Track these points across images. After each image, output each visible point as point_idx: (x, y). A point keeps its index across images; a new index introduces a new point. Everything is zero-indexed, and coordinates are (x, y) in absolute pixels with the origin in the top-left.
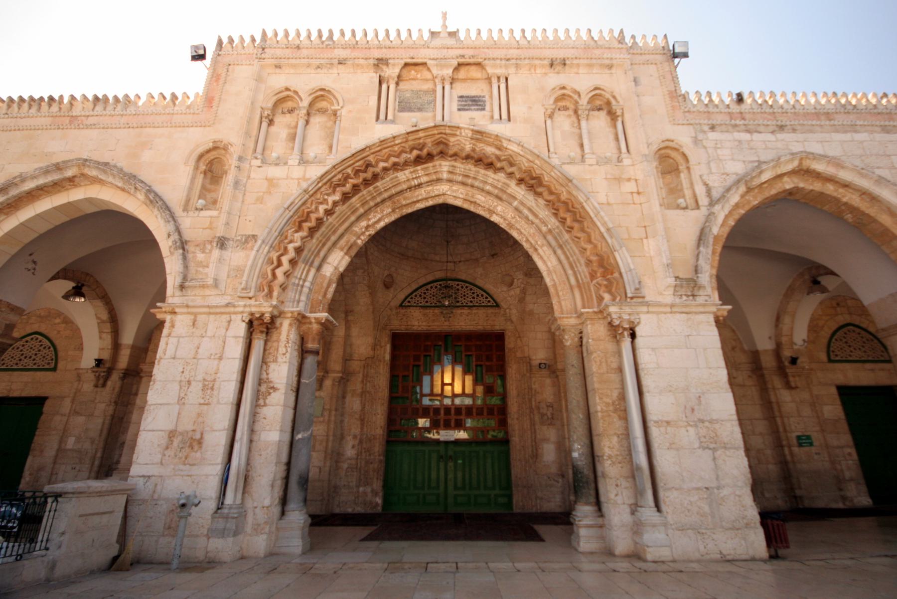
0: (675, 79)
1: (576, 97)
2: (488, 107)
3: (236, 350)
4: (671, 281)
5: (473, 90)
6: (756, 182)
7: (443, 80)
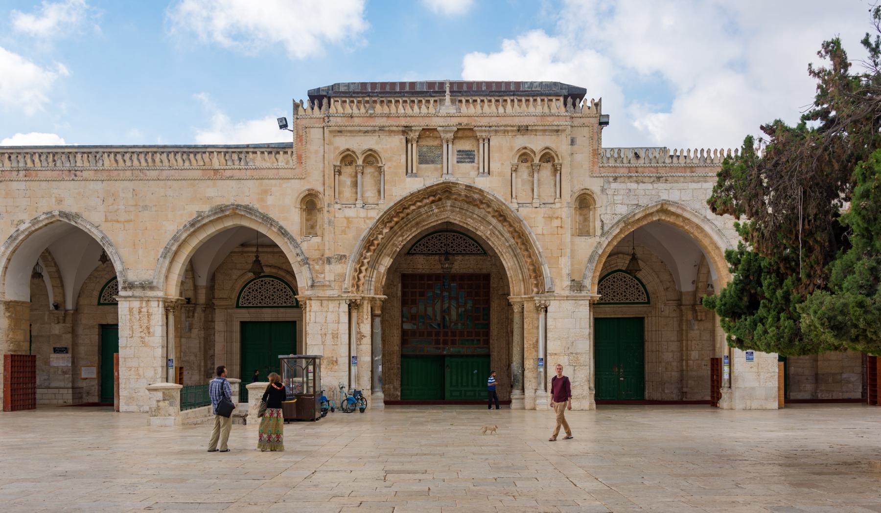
0: (599, 139)
1: (532, 155)
2: (476, 160)
3: (345, 318)
4: (569, 283)
6: (633, 219)
7: (447, 142)
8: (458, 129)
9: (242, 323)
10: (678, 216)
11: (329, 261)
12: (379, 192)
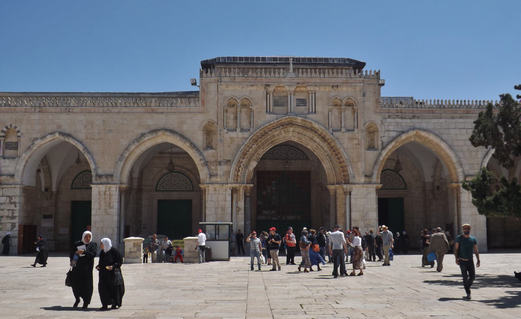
0: (379, 93)
1: (340, 102)
2: (307, 105)
3: (229, 198)
5: (302, 97)
7: (291, 93)
8: (297, 87)
9: (159, 200)
10: (426, 138)
11: (220, 163)
12: (250, 123)
